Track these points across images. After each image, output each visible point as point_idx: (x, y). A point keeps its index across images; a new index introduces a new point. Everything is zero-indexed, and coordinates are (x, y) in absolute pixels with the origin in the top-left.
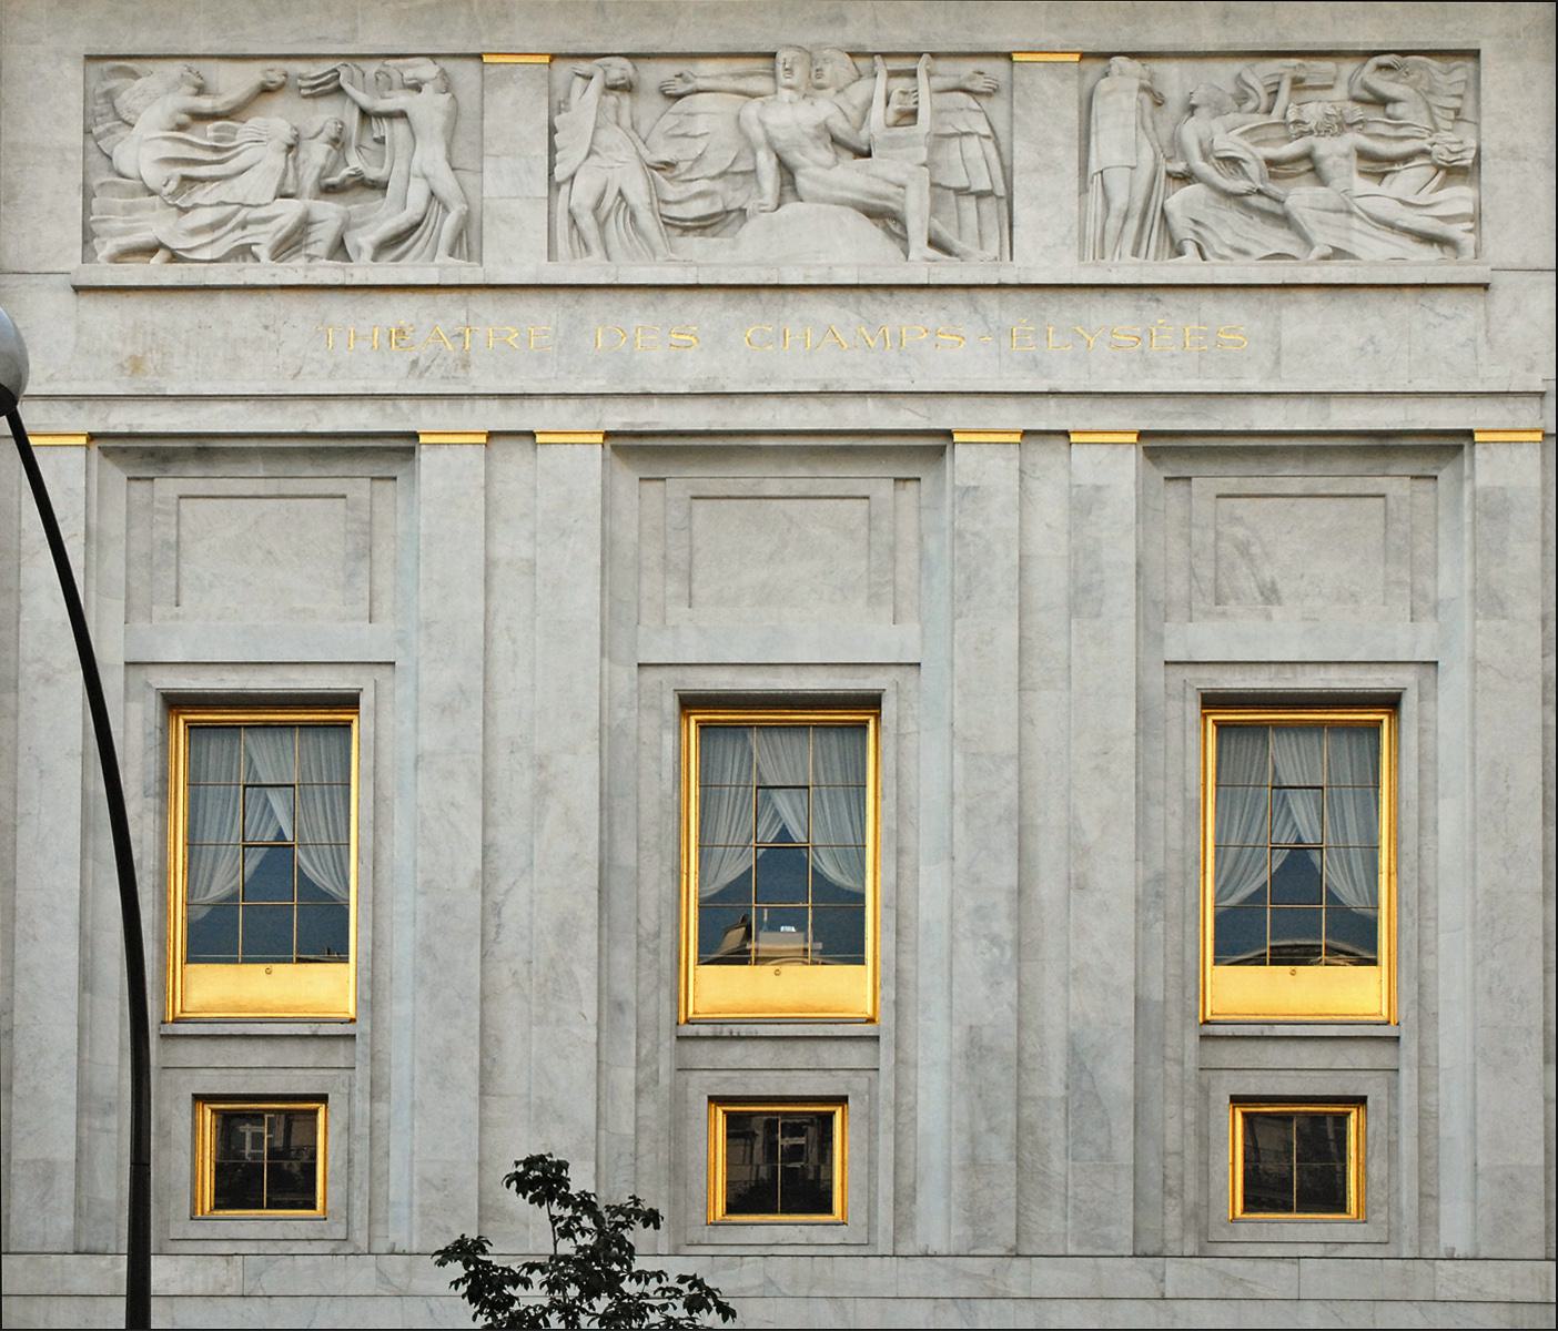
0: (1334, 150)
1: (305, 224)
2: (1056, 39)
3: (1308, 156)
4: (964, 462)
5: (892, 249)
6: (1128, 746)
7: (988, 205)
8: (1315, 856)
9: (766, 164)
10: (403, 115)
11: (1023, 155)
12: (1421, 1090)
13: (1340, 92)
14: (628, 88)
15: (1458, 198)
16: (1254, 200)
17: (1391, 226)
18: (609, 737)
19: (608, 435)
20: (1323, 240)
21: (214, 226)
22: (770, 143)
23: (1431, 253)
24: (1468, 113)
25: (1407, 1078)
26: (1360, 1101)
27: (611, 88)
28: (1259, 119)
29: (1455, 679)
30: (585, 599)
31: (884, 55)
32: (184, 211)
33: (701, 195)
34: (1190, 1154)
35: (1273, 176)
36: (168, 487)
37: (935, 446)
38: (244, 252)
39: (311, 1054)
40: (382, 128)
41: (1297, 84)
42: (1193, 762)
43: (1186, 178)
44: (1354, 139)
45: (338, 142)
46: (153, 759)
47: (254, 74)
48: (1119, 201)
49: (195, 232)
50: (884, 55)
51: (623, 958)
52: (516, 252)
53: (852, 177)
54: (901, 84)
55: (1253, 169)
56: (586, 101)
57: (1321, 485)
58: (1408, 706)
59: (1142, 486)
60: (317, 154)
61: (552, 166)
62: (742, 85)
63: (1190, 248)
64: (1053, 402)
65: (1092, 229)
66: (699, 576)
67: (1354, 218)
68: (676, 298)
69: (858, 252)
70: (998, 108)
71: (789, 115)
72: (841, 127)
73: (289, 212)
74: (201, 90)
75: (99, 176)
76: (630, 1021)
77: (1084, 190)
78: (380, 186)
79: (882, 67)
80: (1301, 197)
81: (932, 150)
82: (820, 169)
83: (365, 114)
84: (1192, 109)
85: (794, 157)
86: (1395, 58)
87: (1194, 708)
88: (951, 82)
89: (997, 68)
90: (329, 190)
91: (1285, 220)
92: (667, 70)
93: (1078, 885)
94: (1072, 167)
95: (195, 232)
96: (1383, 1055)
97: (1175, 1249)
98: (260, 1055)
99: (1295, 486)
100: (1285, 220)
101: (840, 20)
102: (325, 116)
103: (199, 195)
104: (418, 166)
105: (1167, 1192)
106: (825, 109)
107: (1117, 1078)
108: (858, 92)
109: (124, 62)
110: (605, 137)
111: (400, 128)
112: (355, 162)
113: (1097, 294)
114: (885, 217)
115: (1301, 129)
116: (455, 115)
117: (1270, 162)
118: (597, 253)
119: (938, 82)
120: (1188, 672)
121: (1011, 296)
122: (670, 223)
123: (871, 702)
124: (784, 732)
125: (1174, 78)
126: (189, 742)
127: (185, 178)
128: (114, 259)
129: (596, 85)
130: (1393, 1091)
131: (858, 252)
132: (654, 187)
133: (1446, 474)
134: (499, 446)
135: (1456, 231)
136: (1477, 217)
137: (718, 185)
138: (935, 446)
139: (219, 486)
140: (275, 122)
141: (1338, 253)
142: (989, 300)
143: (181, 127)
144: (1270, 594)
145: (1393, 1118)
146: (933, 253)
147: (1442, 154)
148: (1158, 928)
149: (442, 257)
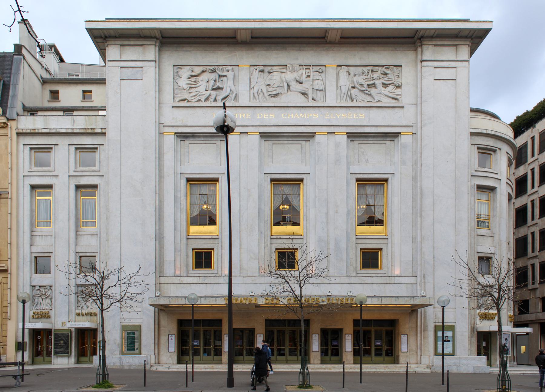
0: (378, 83)
1: (210, 95)
2: (333, 63)
3: (374, 84)
4: (318, 138)
5: (306, 100)
6: (345, 188)
7: (322, 92)
8: (373, 208)
9: (285, 85)
10: (226, 76)
11: (327, 83)
12: (392, 247)
13: (379, 72)
14: (262, 71)
15: (398, 91)
16: (366, 92)
17: (387, 96)
18: (260, 186)
19: (260, 133)
20: (377, 99)
21: (195, 96)
22: (286, 81)
24: (400, 76)
25: (389, 245)
26: (381, 249)
27: (260, 71)
28: (366, 77)
29: (397, 175)
30: (256, 162)
31: (305, 66)
32: (190, 93)
33: (275, 90)
34: (354, 259)
35: (368, 87)
36: (187, 142)
37: (312, 135)
38: (200, 100)
39: (211, 241)
40: (222, 78)
41: (372, 71)
42: (354, 191)
43: (353, 87)
44: (382, 81)
45: (215, 81)
46: (185, 190)
47: (201, 69)
48: (343, 92)
49: (192, 97)
50: (305, 66)
51: (262, 225)
52: (244, 100)
53: (300, 88)
54: (308, 70)
55: (366, 86)
56: (256, 73)
57: (376, 142)
58: (389, 181)
59: (347, 141)
60: (212, 83)
61: (250, 85)
62: (281, 71)
63: (355, 100)
64: (332, 127)
65: (339, 97)
66: (274, 158)
67: (381, 94)
68: (271, 109)
69: (301, 101)
70: (323, 75)
71: (289, 76)
72: (298, 78)
73: (207, 93)
74: (192, 71)
75: (176, 88)
76: (263, 235)
77: (337, 89)
78: (222, 89)
79: (305, 67)
80: (373, 91)
81: (313, 82)
82: (295, 86)
83: (220, 76)
84: (355, 75)
85: (290, 84)
86: (388, 67)
87: (355, 181)
88: (315, 70)
89: (323, 68)
90: (213, 89)
91: (370, 95)
92: (269, 68)
93: (336, 212)
94: (335, 86)
95: (192, 97)
96: (385, 241)
97: (352, 275)
98: (203, 241)
99: (371, 142)
100: (370, 95)
101: (297, 59)
102: (214, 76)
103: (193, 90)
104: (228, 85)
105: (350, 265)
106: (295, 75)
107: (343, 245)
108: (300, 72)
109: (179, 66)
110: (259, 80)
111: (225, 78)
112: (218, 84)
113: (339, 108)
115: (373, 79)
116: (234, 76)
117: (368, 85)
118: (258, 101)
119: (314, 70)
120: (353, 175)
121: (325, 108)
122: (269, 95)
123: (302, 180)
124: (287, 185)
125: (351, 69)
126: (190, 187)
127: (190, 87)
128: (179, 101)
129: (258, 70)
130: (387, 247)
131: (301, 101)
132: (267, 89)
133: (396, 140)
134: (242, 134)
135: (398, 97)
137: (277, 89)
138: (312, 135)
139: (195, 142)
140: (205, 76)
141: (379, 101)
142: (322, 109)
143: (189, 78)
144: (367, 161)
145: (387, 252)
146: (313, 101)
147: (396, 84)
148: (349, 219)
149: (233, 101)
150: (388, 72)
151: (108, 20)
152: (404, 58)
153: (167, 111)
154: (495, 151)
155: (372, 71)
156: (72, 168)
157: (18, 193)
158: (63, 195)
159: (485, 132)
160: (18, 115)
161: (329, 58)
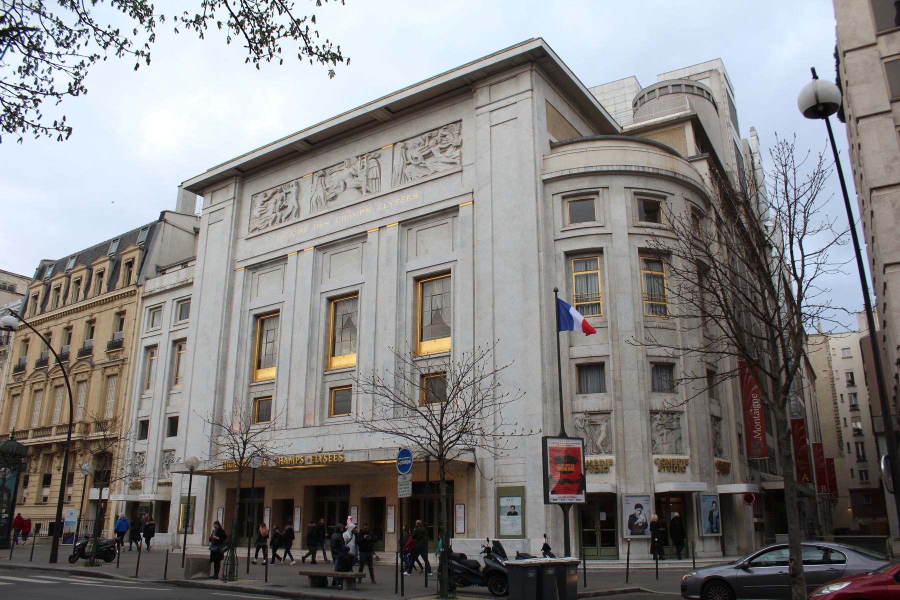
1: (276, 217)
9: (342, 184)
14: (323, 176)
23: (453, 166)
38: (268, 225)
43: (410, 164)
45: (282, 200)
57: (435, 224)
67: (439, 164)
71: (346, 172)
72: (353, 172)
80: (428, 162)
86: (446, 127)
114: (359, 188)
124: (342, 301)
128: (252, 231)
132: (324, 194)
136: (461, 155)
141: (435, 172)
144: (427, 251)
147: (454, 144)
150: (445, 133)
151: (209, 171)
152: (460, 111)
153: (242, 243)
154: (597, 193)
155: (430, 138)
156: (172, 324)
157: (135, 356)
158: (164, 353)
159: (567, 173)
160: (147, 279)
161: (384, 141)
